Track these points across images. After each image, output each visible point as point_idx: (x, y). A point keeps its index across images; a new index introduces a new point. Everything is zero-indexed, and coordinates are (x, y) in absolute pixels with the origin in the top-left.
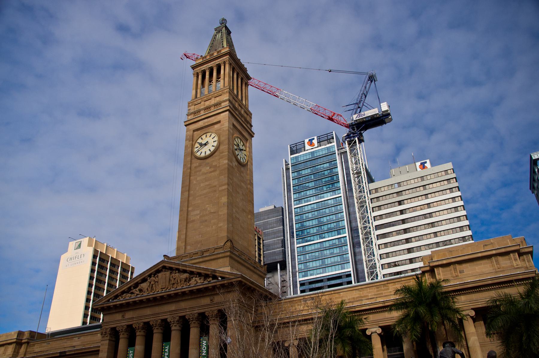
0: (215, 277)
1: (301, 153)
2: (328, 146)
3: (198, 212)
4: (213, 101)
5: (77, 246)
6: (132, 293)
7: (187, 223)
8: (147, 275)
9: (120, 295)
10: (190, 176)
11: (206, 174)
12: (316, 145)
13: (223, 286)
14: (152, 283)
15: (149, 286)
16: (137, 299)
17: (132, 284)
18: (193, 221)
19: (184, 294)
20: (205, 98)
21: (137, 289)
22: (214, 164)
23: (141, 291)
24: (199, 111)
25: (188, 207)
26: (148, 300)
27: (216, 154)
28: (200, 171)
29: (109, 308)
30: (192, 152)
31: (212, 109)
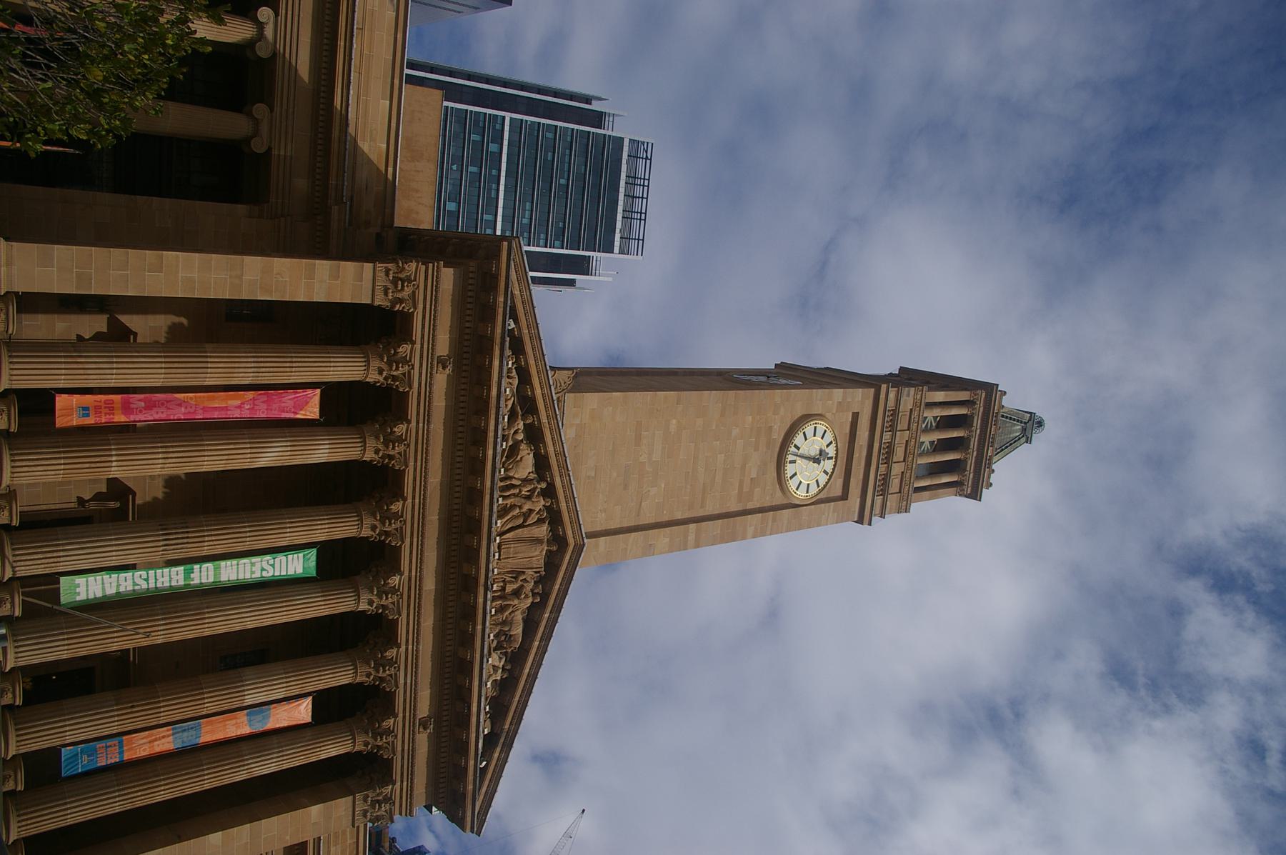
0: (491, 740)
2: (618, 236)
4: (897, 469)
6: (513, 416)
8: (558, 480)
9: (517, 362)
11: (743, 467)
13: (461, 773)
17: (544, 420)
18: (638, 439)
19: (467, 640)
21: (520, 437)
23: (513, 450)
24: (893, 429)
26: (474, 496)
28: (756, 449)
29: (487, 314)
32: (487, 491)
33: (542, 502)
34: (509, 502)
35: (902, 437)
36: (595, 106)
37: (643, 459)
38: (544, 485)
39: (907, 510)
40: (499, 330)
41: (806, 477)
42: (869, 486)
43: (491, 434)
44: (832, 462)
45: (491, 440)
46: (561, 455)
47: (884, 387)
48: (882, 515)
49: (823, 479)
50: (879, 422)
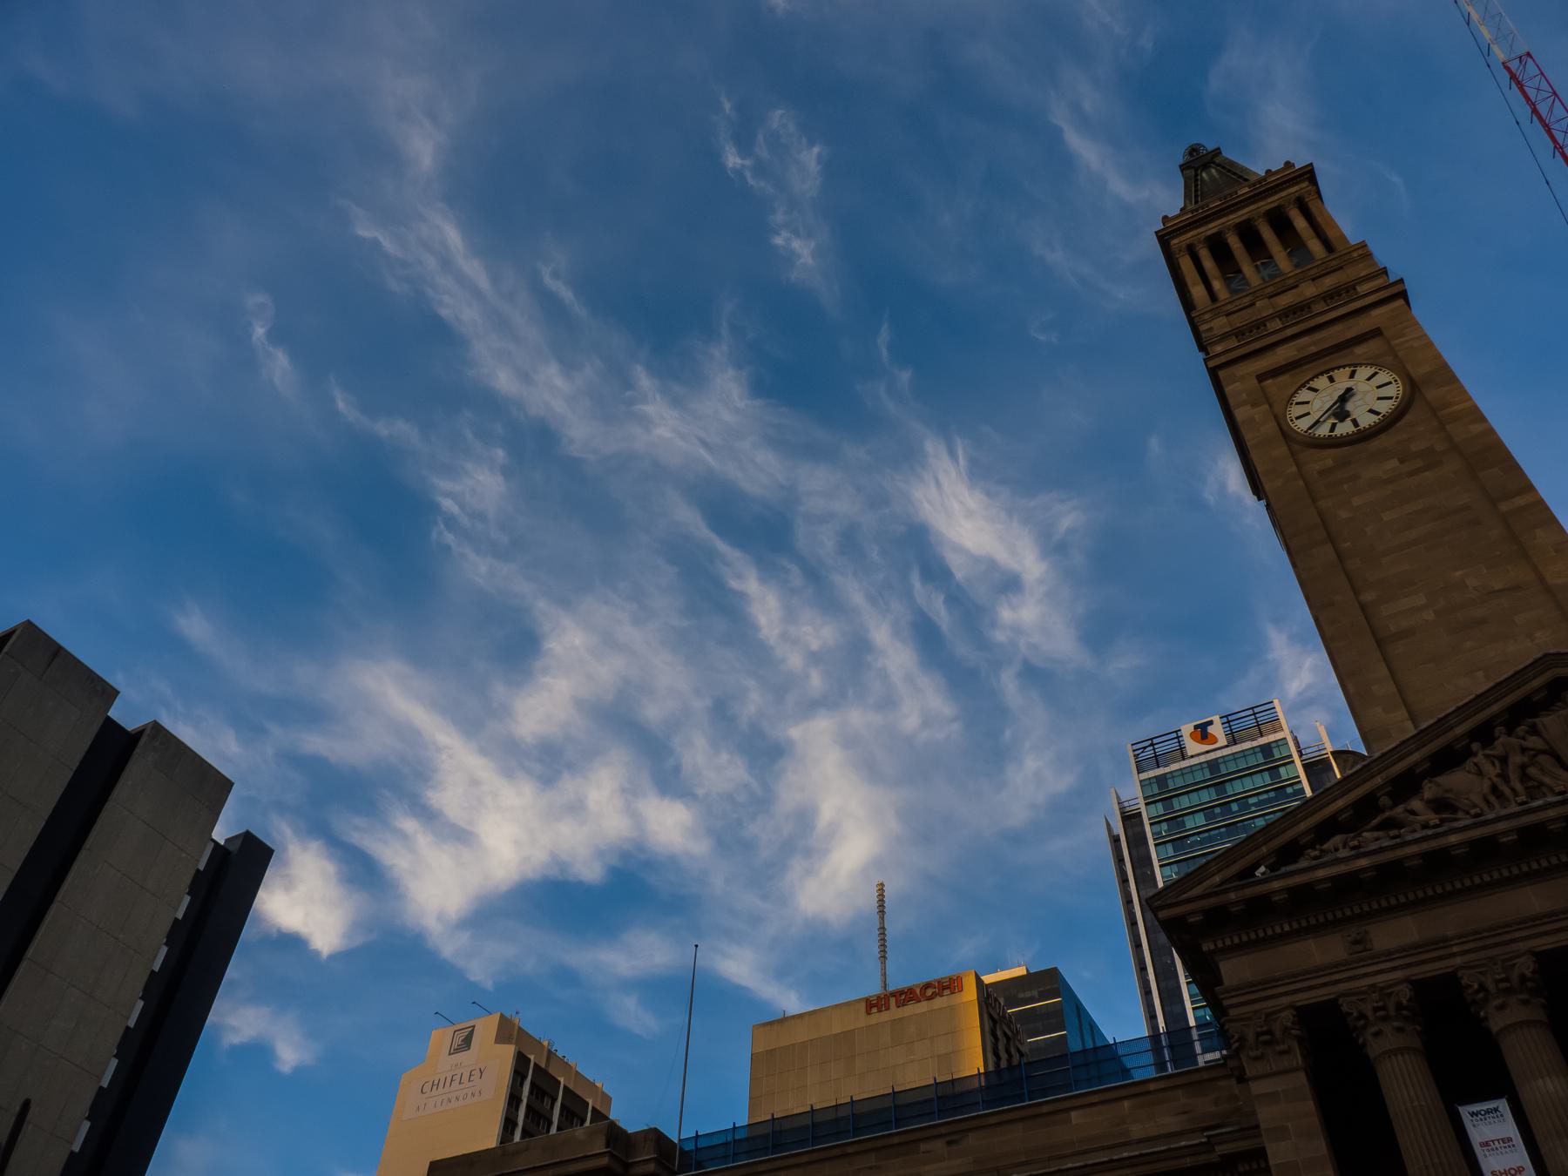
1: (1175, 767)
3: (1420, 600)
4: (1309, 290)
5: (458, 1040)
7: (1379, 643)
8: (1460, 730)
9: (1312, 846)
10: (1314, 501)
12: (1222, 741)
14: (1517, 759)
15: (1504, 776)
16: (1453, 839)
17: (1379, 780)
20: (1268, 290)
21: (1416, 804)
22: (1414, 447)
23: (1442, 805)
24: (1260, 324)
25: (1356, 592)
27: (1408, 418)
29: (1260, 909)
30: (1286, 434)
31: (1319, 307)
32: (1515, 823)
33: (1503, 739)
34: (1518, 786)
35: (1263, 308)
36: (1119, 829)
37: (1429, 615)
38: (1475, 746)
39: (1363, 245)
40: (1276, 885)
41: (1372, 394)
42: (1355, 306)
43: (1425, 846)
44: (1335, 374)
45: (1434, 844)
46: (1421, 737)
47: (1212, 364)
48: (1384, 271)
49: (1363, 372)
50: (1257, 345)
